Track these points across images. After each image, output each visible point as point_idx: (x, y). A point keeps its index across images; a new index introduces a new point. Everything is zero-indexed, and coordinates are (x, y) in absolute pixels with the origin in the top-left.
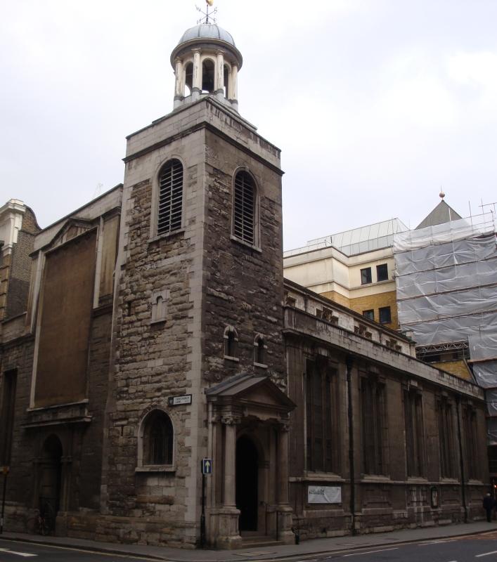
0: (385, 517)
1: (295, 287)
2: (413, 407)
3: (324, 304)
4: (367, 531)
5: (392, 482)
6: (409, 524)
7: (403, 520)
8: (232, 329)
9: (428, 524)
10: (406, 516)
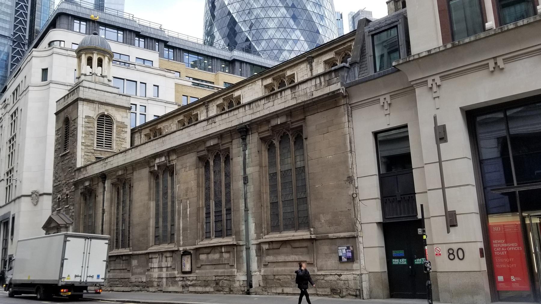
0: (123, 280)
1: (195, 104)
2: (169, 178)
3: (221, 96)
4: (109, 289)
5: (131, 253)
6: (148, 287)
7: (142, 284)
8: (59, 196)
9: (171, 289)
10: (144, 281)
